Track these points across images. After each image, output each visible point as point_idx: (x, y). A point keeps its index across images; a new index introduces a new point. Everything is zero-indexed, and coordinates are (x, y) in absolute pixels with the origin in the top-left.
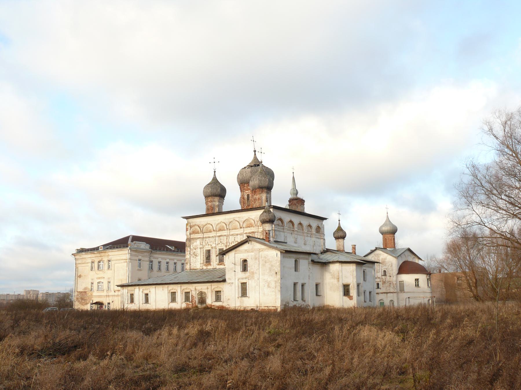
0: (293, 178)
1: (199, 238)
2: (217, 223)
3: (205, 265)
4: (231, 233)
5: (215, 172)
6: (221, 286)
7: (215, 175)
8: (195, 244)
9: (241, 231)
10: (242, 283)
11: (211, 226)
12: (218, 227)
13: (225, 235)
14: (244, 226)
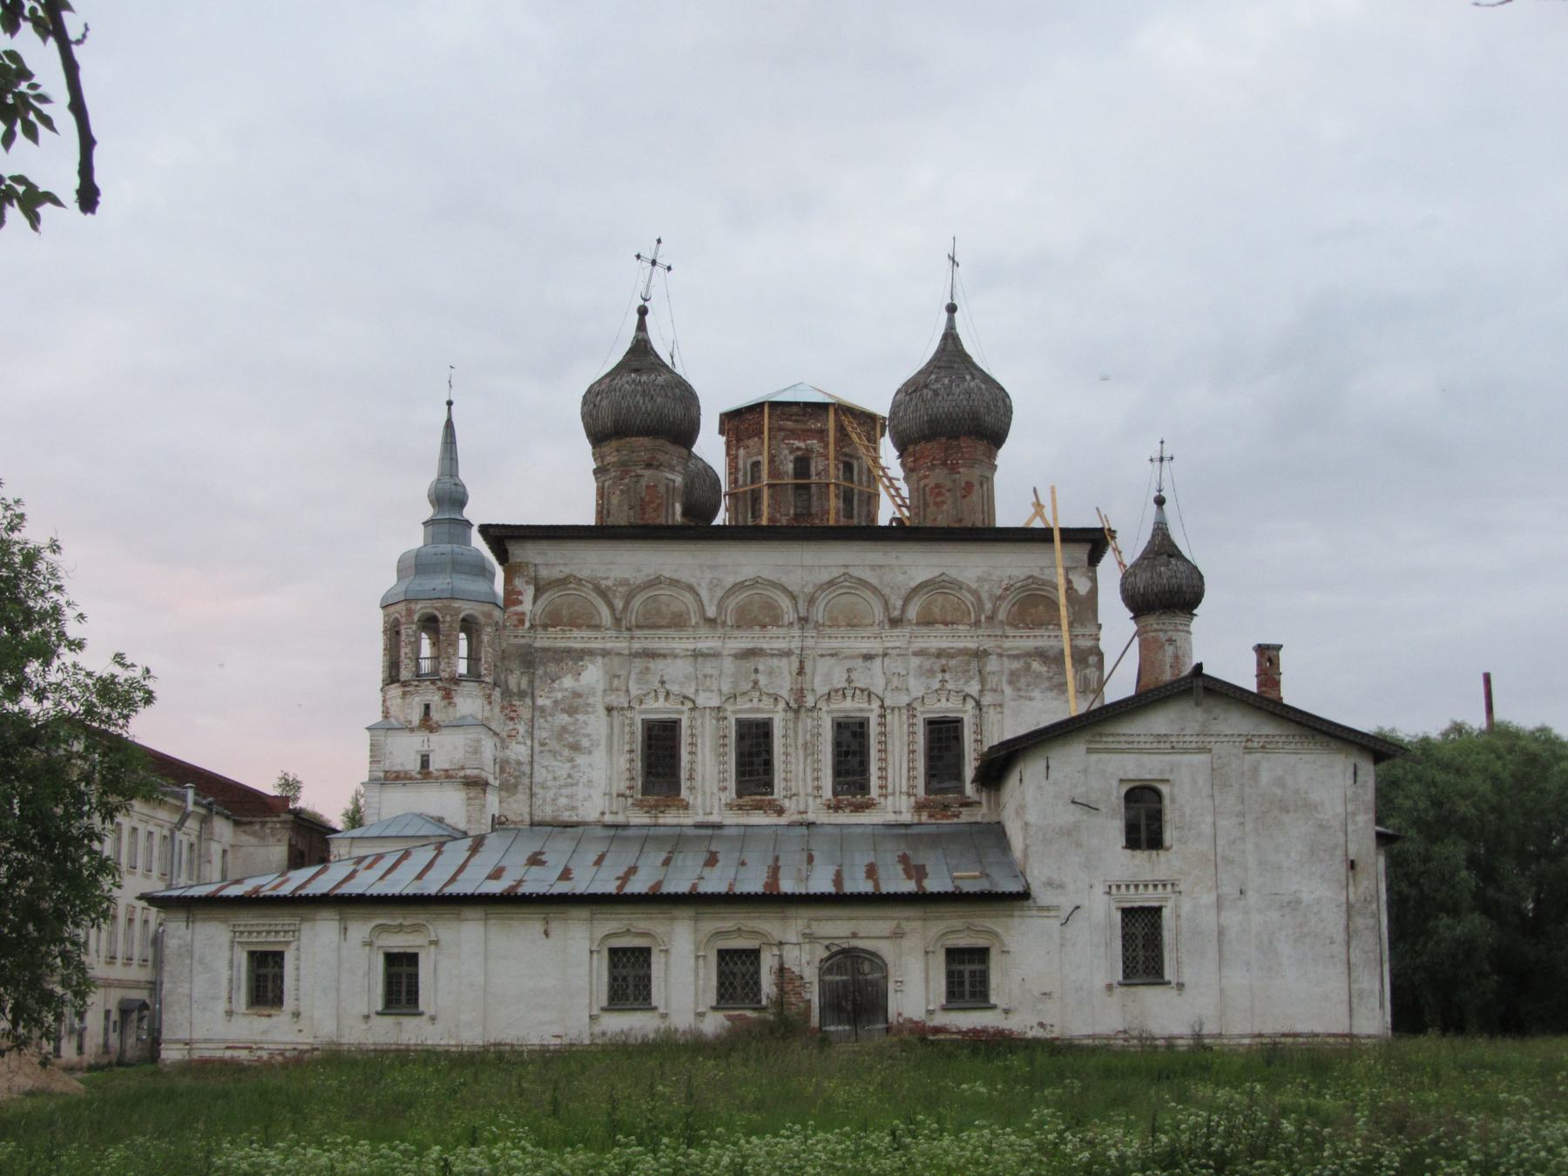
0: (449, 425)
1: (605, 653)
2: (729, 581)
3: (639, 805)
4: (827, 644)
5: (643, 312)
6: (989, 923)
7: (642, 326)
8: (568, 682)
9: (896, 639)
10: (1127, 912)
11: (688, 597)
12: (732, 603)
13: (787, 654)
14: (912, 613)
